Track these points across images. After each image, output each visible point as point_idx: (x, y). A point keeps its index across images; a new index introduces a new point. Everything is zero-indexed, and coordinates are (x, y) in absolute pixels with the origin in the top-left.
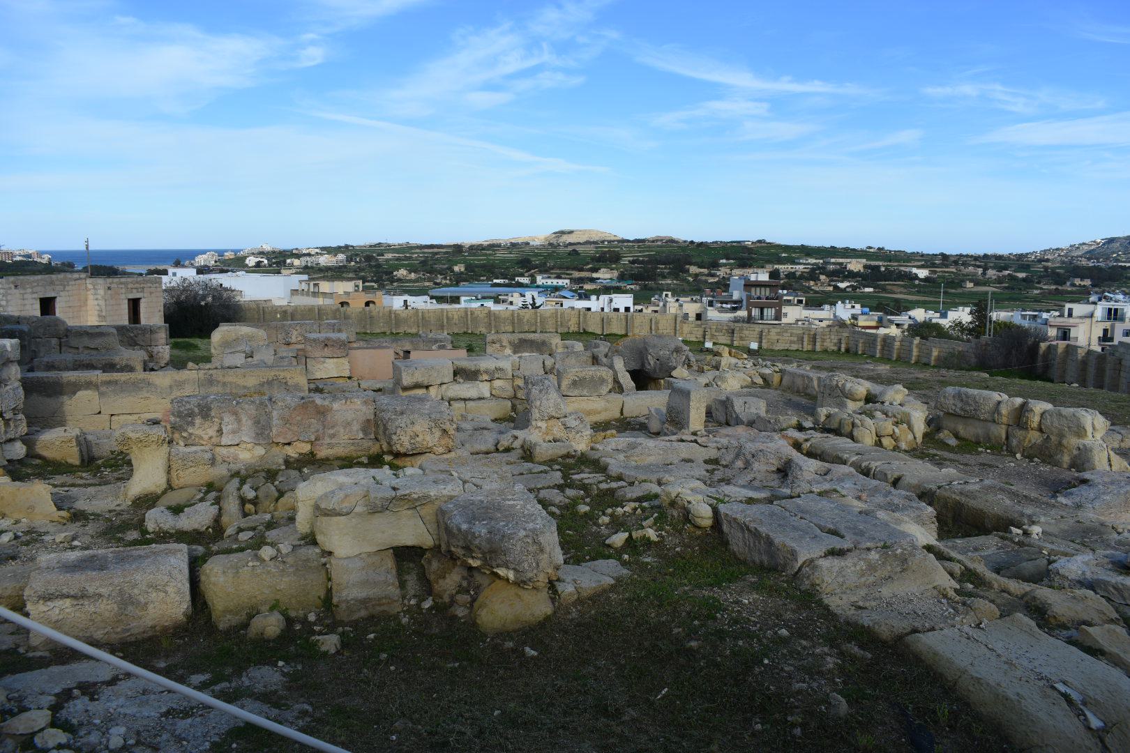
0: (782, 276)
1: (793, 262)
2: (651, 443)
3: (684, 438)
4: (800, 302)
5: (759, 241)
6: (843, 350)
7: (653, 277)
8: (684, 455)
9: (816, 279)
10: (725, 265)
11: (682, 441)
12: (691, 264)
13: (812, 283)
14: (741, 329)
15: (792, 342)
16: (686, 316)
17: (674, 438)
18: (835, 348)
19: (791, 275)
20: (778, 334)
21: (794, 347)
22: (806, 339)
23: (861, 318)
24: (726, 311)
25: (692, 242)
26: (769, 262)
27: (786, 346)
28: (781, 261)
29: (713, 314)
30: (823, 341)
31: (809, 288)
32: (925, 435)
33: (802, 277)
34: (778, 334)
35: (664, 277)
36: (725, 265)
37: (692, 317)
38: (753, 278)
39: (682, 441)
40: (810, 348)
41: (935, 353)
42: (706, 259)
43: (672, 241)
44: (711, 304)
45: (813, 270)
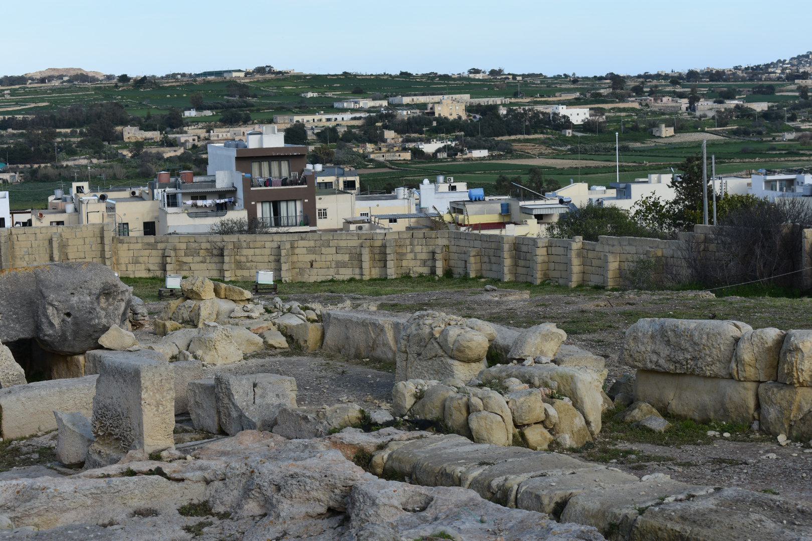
0: (310, 136)
1: (330, 108)
2: (66, 485)
3: (134, 466)
4: (350, 185)
5: (260, 70)
6: (440, 272)
7: (47, 155)
8: (137, 503)
9: (377, 139)
10: (194, 121)
11: (132, 473)
12: (124, 123)
13: (370, 147)
14: (237, 247)
15: (340, 265)
16: (124, 228)
17: (113, 469)
18: (425, 270)
19: (328, 135)
20: (311, 250)
21: (345, 274)
22: (366, 257)
23: (470, 208)
24: (204, 213)
25: (124, 78)
26: (282, 110)
27: (330, 274)
28: (305, 108)
29: (178, 221)
30: (400, 257)
31: (365, 156)
32: (607, 416)
33: (349, 136)
34: (311, 250)
35: (71, 152)
36: (194, 121)
37: (136, 229)
38: (253, 143)
39: (132, 473)
40: (376, 273)
41: (613, 265)
42: (157, 111)
43: (83, 77)
44: (172, 201)
45: (370, 122)
